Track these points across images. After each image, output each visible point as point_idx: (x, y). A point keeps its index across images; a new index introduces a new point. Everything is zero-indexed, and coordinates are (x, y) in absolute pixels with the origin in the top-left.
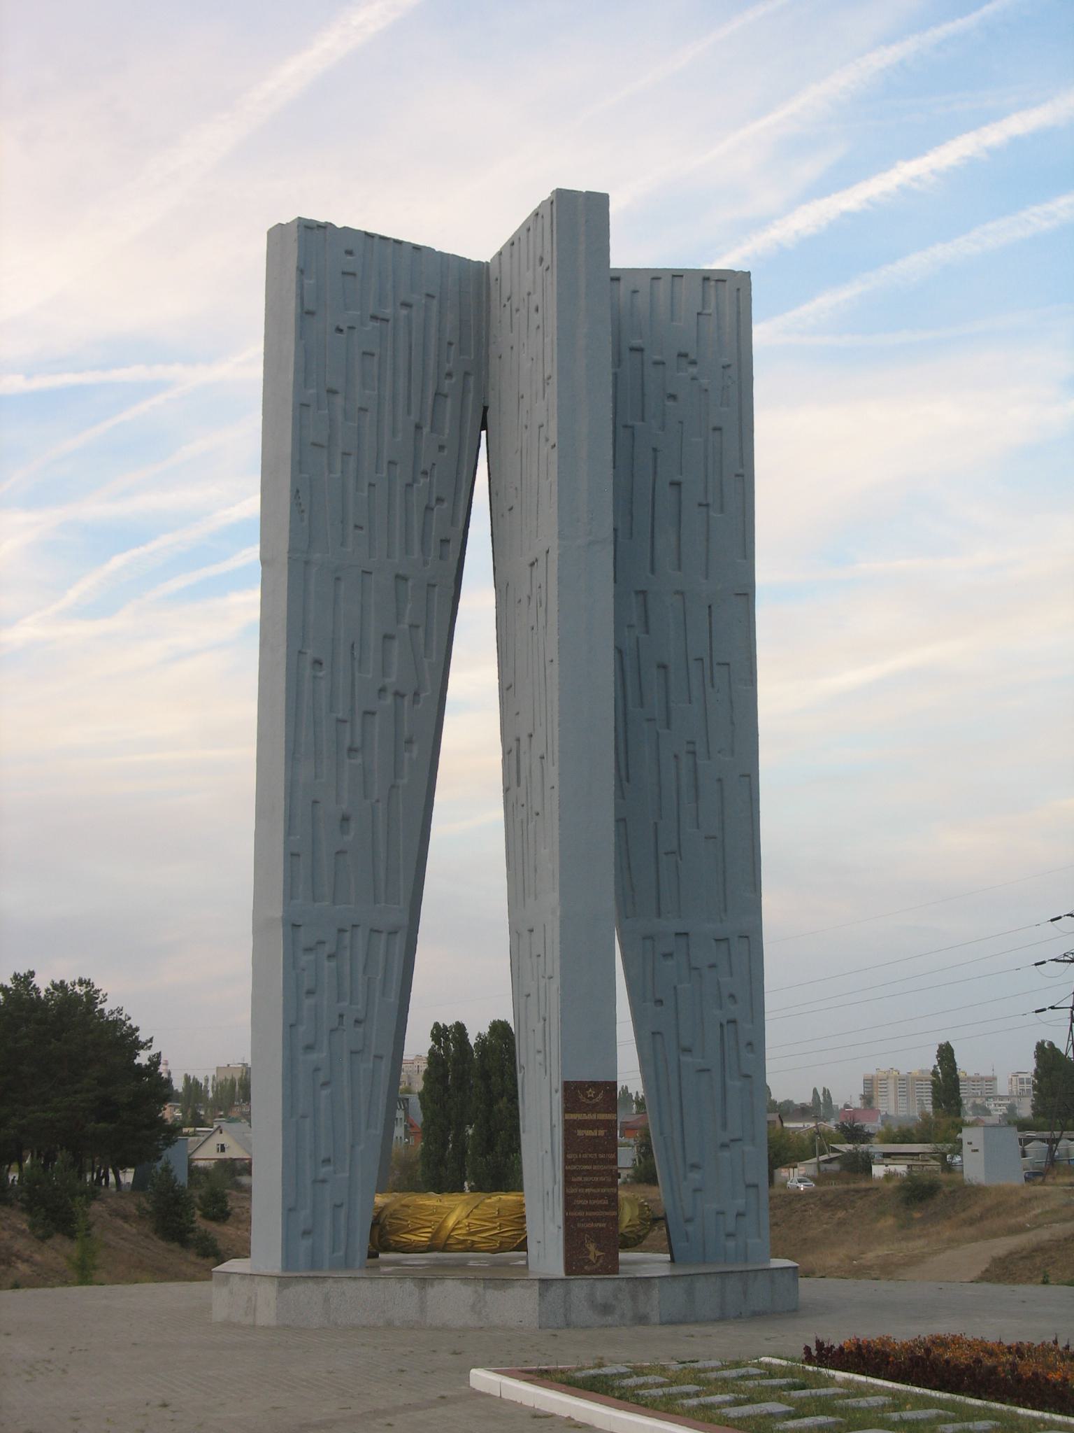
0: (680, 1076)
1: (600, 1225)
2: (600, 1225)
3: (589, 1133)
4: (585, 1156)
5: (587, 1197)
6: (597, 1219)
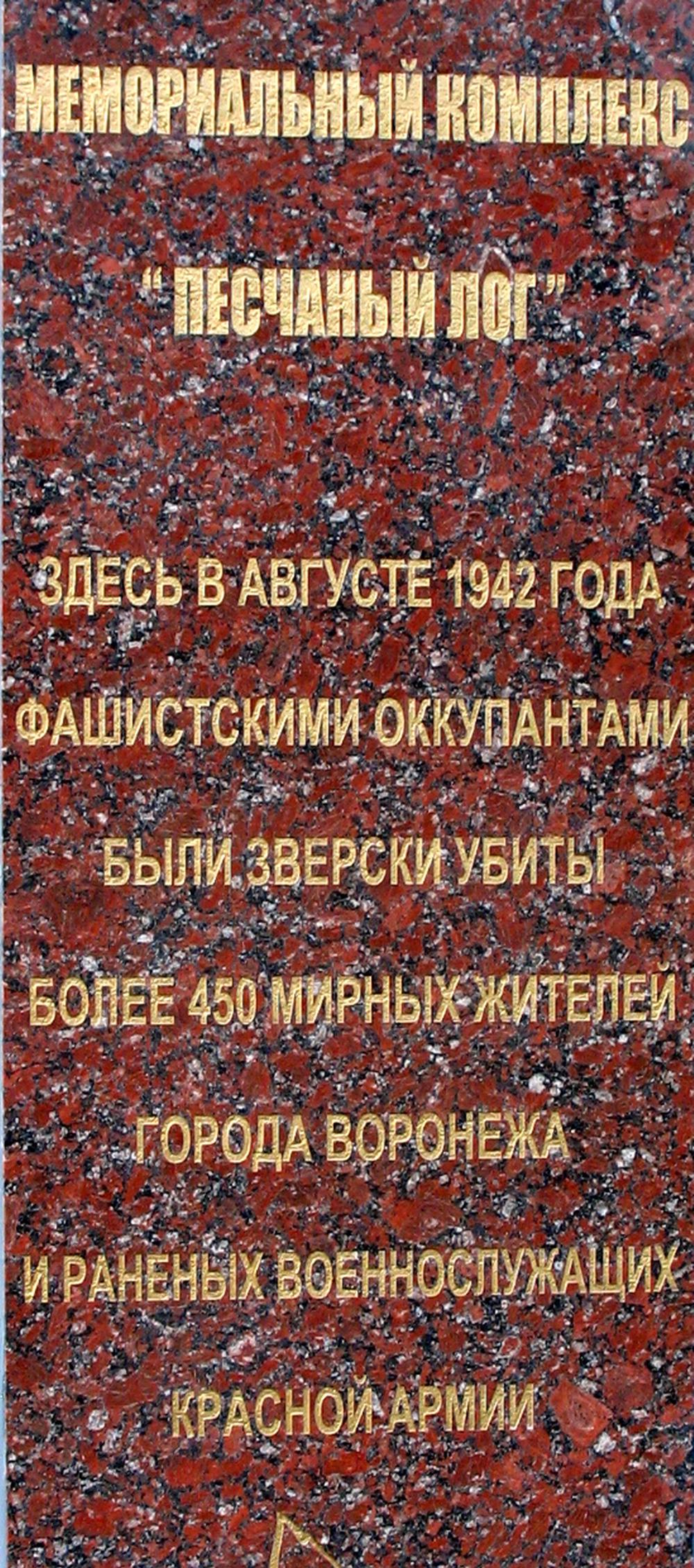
0: (357, 289)
1: (463, 1406)
2: (463, 1406)
3: (326, 304)
4: (280, 585)
5: (288, 1070)
6: (433, 1343)
